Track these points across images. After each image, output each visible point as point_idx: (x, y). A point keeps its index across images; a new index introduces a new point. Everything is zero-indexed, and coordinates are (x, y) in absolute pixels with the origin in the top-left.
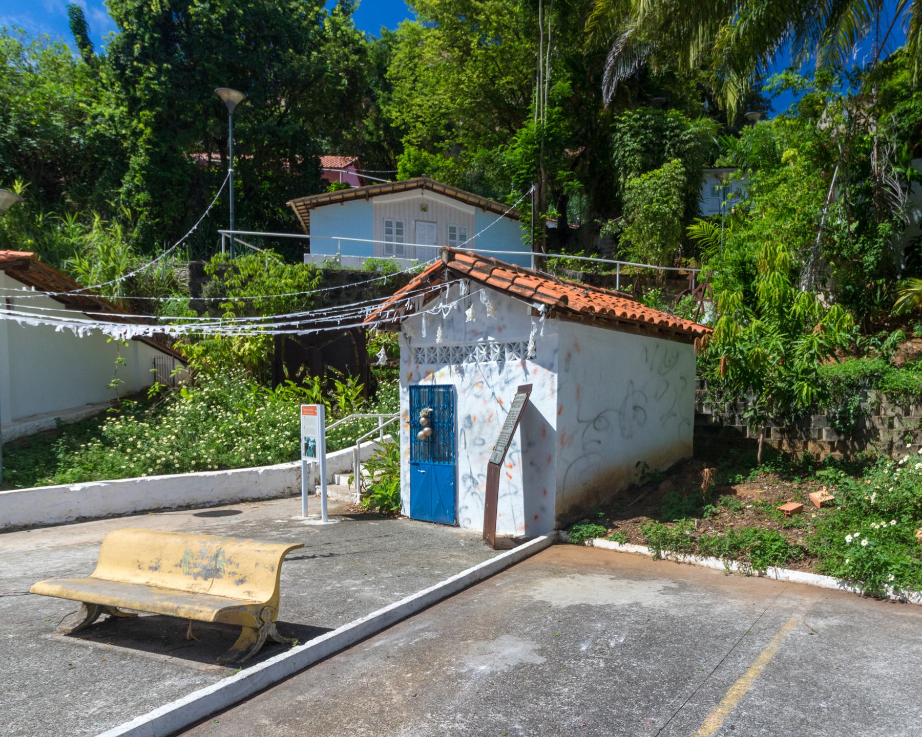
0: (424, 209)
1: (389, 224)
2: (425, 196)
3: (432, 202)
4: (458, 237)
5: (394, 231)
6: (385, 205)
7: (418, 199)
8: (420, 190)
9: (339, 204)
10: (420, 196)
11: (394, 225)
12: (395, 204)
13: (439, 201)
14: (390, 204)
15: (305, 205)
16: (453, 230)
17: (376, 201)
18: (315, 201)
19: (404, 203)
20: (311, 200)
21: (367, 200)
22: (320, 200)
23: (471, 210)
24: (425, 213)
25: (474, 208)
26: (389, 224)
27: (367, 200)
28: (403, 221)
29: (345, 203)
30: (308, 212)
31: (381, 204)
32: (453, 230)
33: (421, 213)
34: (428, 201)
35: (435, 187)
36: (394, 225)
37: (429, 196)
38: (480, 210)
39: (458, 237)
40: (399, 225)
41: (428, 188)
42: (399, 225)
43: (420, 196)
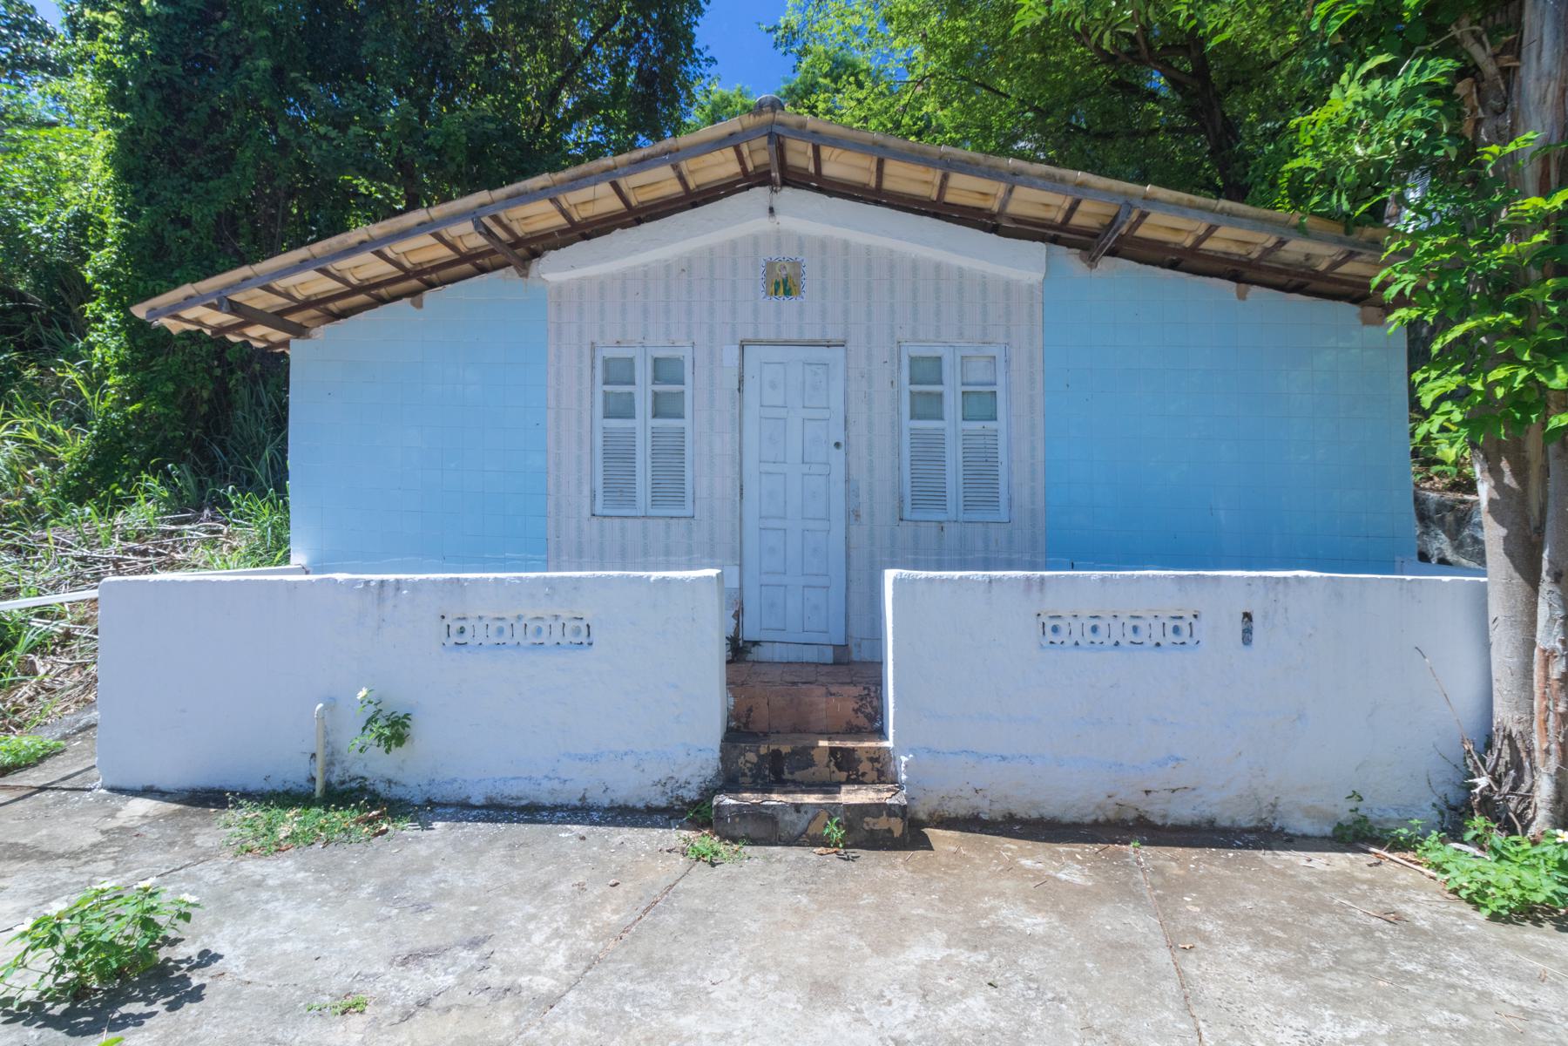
0: (784, 285)
1: (618, 372)
2: (785, 221)
3: (823, 245)
4: (952, 404)
5: (643, 405)
7: (755, 240)
8: (760, 194)
9: (406, 301)
10: (763, 224)
11: (643, 373)
13: (858, 238)
16: (926, 370)
19: (686, 267)
23: (1022, 265)
25: (1040, 247)
26: (618, 372)
28: (685, 353)
32: (926, 370)
33: (769, 305)
34: (801, 242)
35: (838, 165)
36: (643, 373)
38: (1069, 259)
39: (952, 404)
40: (665, 370)
41: (793, 179)
42: (665, 370)
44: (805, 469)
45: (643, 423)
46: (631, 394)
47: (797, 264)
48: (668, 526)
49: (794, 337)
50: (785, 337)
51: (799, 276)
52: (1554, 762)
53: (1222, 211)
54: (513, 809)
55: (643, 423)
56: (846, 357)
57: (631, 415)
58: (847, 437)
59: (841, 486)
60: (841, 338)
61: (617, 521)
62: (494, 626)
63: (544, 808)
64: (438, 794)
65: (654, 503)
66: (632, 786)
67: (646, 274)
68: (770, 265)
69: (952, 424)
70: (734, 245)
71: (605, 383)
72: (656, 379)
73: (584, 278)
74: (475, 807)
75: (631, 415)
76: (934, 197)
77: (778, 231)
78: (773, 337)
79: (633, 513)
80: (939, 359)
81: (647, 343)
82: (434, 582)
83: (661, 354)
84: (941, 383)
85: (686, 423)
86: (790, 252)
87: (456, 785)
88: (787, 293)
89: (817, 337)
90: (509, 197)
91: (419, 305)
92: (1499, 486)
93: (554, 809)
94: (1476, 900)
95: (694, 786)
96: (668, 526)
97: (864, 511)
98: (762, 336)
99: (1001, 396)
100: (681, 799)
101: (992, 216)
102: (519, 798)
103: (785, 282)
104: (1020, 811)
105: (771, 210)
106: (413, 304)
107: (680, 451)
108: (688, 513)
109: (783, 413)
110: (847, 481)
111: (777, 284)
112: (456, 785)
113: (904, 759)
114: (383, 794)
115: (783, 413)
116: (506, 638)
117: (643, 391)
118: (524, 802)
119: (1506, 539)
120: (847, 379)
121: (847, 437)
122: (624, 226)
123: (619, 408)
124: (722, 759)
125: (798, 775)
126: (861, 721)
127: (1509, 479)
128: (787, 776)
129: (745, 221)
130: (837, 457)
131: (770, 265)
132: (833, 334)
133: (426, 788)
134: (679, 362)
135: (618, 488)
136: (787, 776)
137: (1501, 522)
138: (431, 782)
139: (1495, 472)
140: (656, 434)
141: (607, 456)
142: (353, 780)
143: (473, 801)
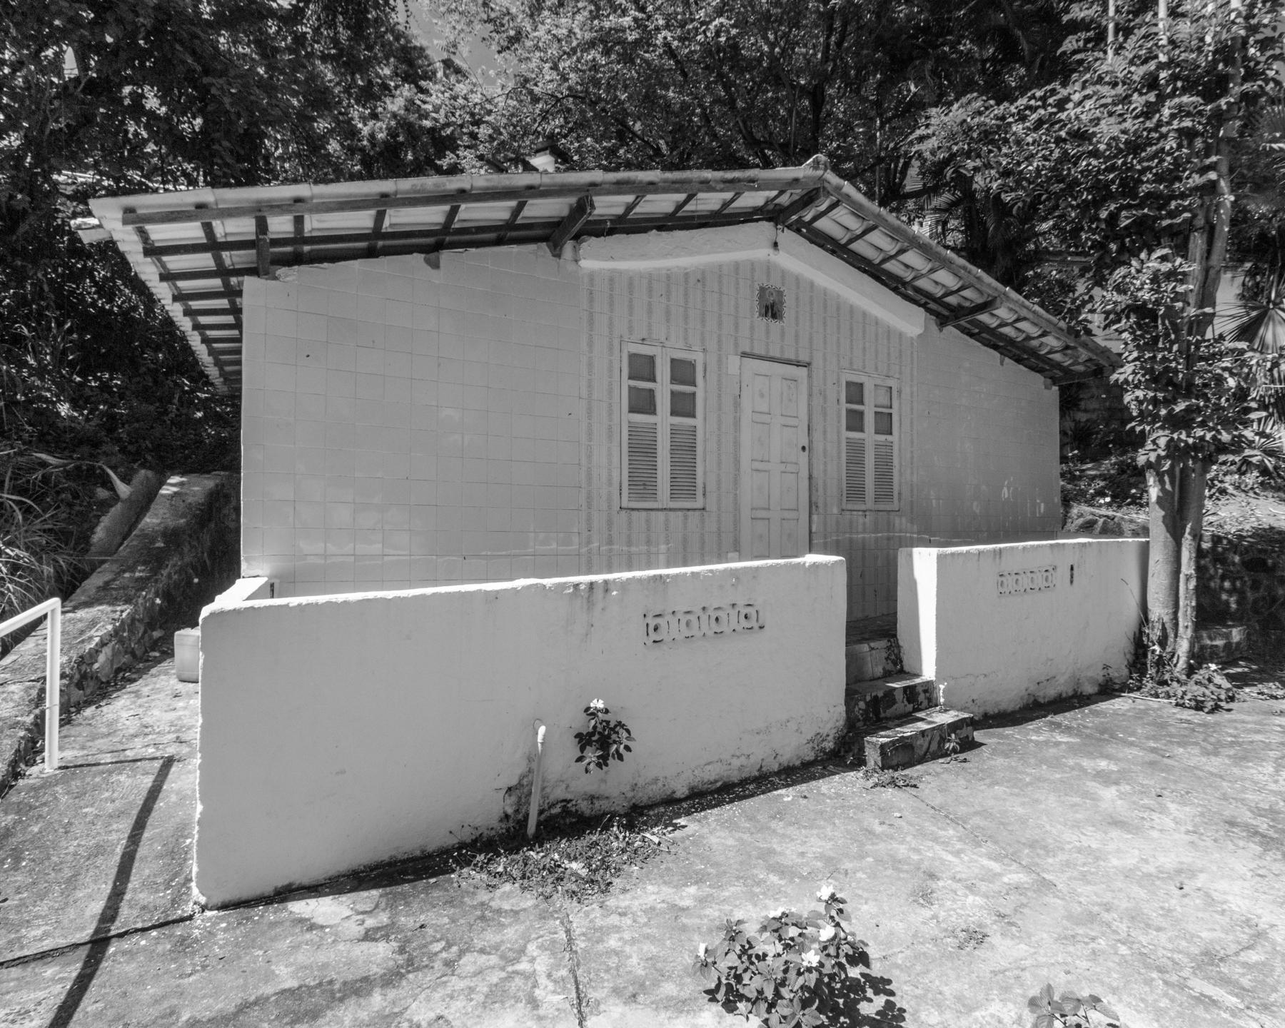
1: (642, 368)
3: (797, 279)
6: (631, 281)
7: (752, 265)
8: (765, 229)
9: (418, 258)
10: (762, 253)
11: (663, 371)
12: (669, 276)
14: (650, 278)
15: (212, 245)
16: (855, 392)
17: (596, 259)
18: (280, 225)
20: (260, 212)
21: (557, 251)
22: (315, 224)
23: (909, 322)
24: (775, 325)
27: (557, 251)
28: (698, 358)
29: (445, 256)
30: (233, 293)
31: (612, 278)
32: (855, 392)
33: (762, 323)
34: (784, 274)
36: (663, 371)
37: (796, 260)
40: (683, 371)
43: (762, 253)
44: (782, 467)
45: (663, 420)
46: (651, 392)
47: (780, 293)
48: (686, 517)
49: (778, 355)
50: (771, 354)
51: (782, 303)
52: (1190, 632)
53: (1034, 312)
54: (712, 793)
55: (663, 420)
56: (810, 376)
57: (652, 411)
58: (810, 442)
59: (806, 482)
60: (807, 360)
61: (644, 514)
62: (684, 619)
63: (734, 785)
64: (642, 797)
65: (673, 496)
66: (793, 747)
67: (668, 277)
68: (762, 290)
69: (869, 436)
70: (737, 266)
71: (630, 378)
72: (674, 380)
73: (613, 271)
74: (679, 801)
75: (652, 411)
76: (877, 261)
77: (769, 262)
78: (763, 353)
79: (655, 505)
80: (862, 385)
81: (667, 344)
82: (640, 580)
83: (679, 355)
84: (862, 403)
85: (698, 422)
86: (775, 282)
87: (660, 784)
88: (774, 316)
89: (793, 357)
90: (618, 183)
91: (436, 265)
92: (1163, 489)
93: (743, 782)
94: (1199, 707)
95: (830, 738)
96: (686, 517)
97: (821, 505)
98: (756, 351)
99: (895, 418)
100: (823, 750)
101: (904, 284)
102: (716, 781)
103: (772, 306)
104: (992, 710)
105: (776, 245)
106: (427, 261)
107: (693, 448)
108: (699, 504)
109: (766, 418)
110: (810, 477)
111: (767, 307)
112: (660, 784)
113: (942, 687)
114: (588, 813)
115: (766, 418)
116: (695, 632)
117: (663, 388)
118: (719, 784)
119: (1164, 517)
120: (810, 395)
121: (810, 442)
122: (660, 228)
123: (643, 403)
124: (847, 712)
125: (889, 712)
126: (890, 666)
127: (1168, 487)
128: (882, 715)
129: (750, 247)
130: (804, 457)
131: (762, 290)
132: (804, 357)
133: (630, 795)
134: (691, 365)
135: (642, 482)
136: (882, 715)
137: (1162, 507)
138: (634, 787)
139: (1162, 482)
140: (674, 431)
141: (632, 450)
142: (552, 806)
143: (678, 795)
